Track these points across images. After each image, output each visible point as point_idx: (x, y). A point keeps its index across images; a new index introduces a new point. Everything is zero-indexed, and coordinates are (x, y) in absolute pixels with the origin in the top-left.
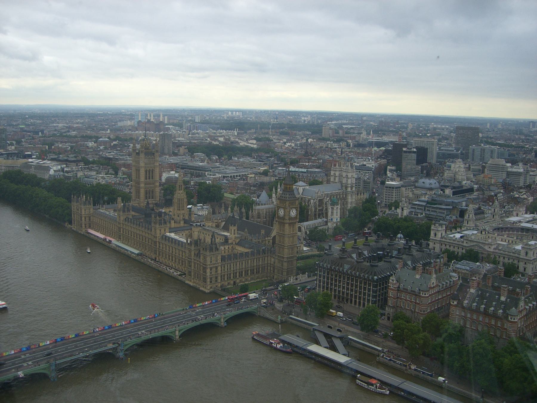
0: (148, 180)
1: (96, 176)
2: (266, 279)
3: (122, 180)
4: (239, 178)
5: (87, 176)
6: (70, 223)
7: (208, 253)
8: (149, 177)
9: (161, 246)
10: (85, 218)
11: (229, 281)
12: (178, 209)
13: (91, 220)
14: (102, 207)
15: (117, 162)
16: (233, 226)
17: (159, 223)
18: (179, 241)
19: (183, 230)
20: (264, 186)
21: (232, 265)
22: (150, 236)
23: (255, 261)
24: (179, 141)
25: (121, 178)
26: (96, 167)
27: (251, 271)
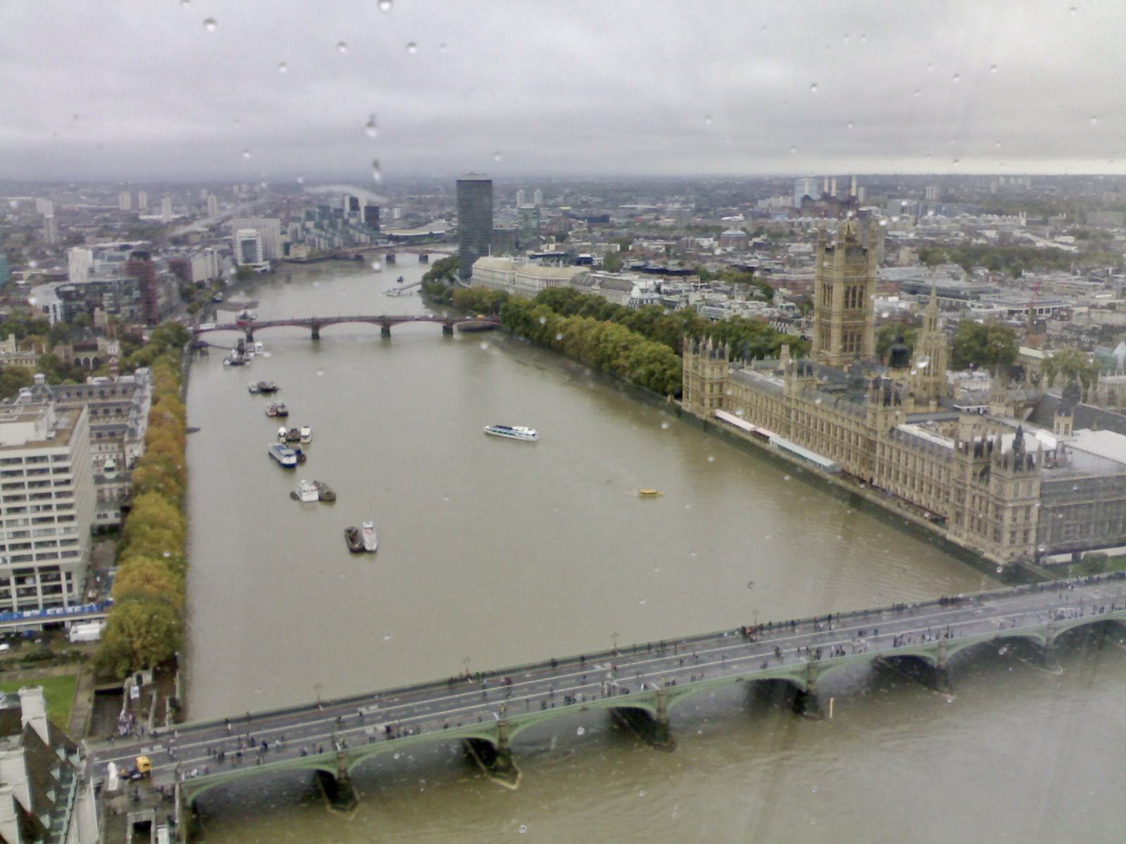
0: (850, 309)
1: (728, 303)
3: (785, 312)
4: (1049, 315)
5: (709, 302)
6: (679, 396)
7: (1009, 473)
8: (854, 302)
10: (712, 386)
14: (749, 363)
15: (769, 277)
16: (1063, 414)
18: (932, 445)
20: (1113, 334)
22: (861, 431)
24: (894, 236)
25: (782, 307)
26: (725, 284)
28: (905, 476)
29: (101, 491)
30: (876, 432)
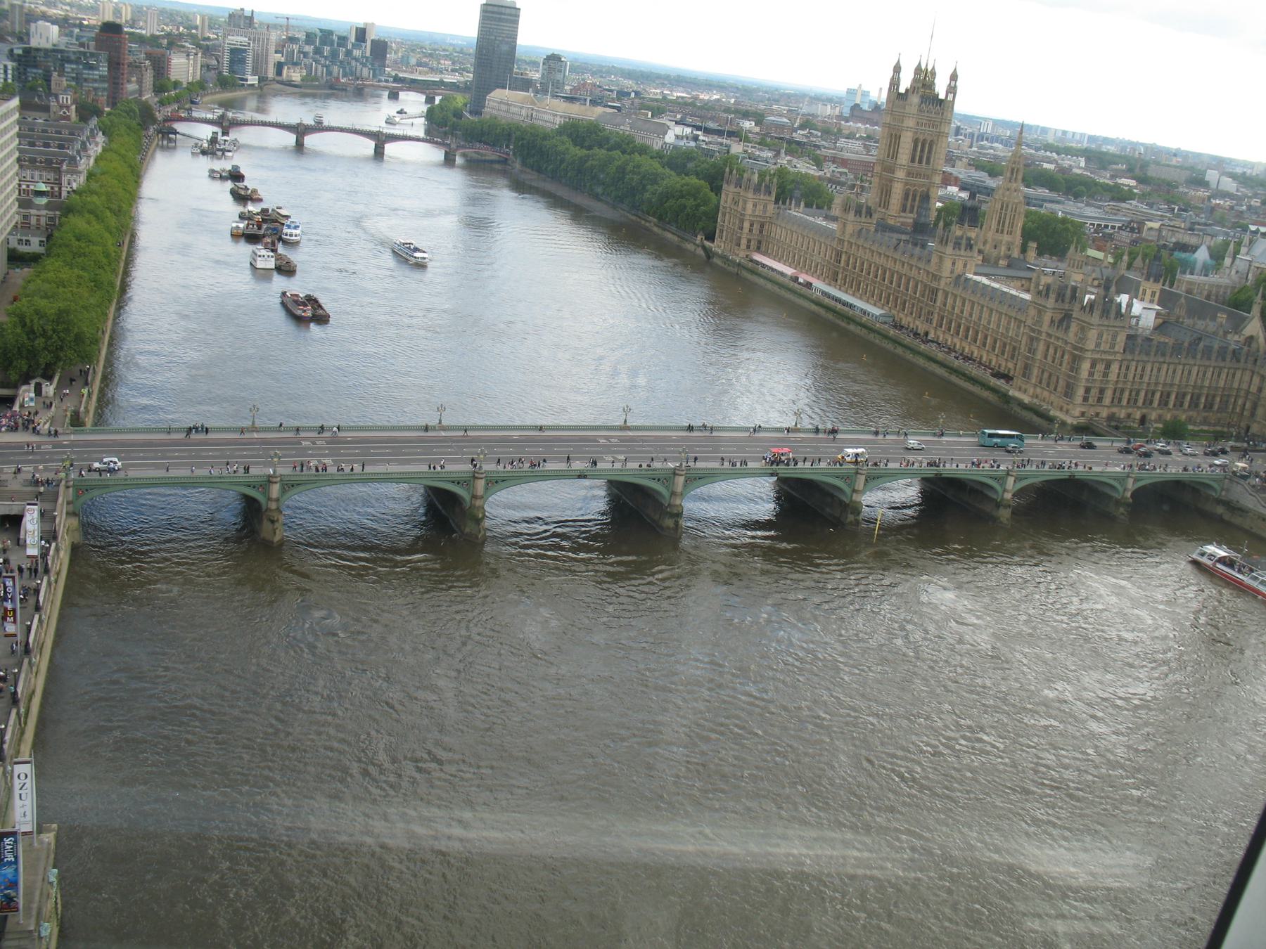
0: (916, 164)
2: (1225, 430)
6: (711, 237)
7: (1095, 319)
9: (950, 301)
10: (752, 225)
11: (1130, 410)
12: (997, 231)
13: (765, 233)
14: (798, 205)
16: (1152, 280)
17: (955, 243)
19: (1007, 277)
21: (1148, 368)
22: (922, 276)
23: (1209, 374)
27: (1191, 398)
28: (967, 330)
29: (26, 217)
30: (936, 277)
